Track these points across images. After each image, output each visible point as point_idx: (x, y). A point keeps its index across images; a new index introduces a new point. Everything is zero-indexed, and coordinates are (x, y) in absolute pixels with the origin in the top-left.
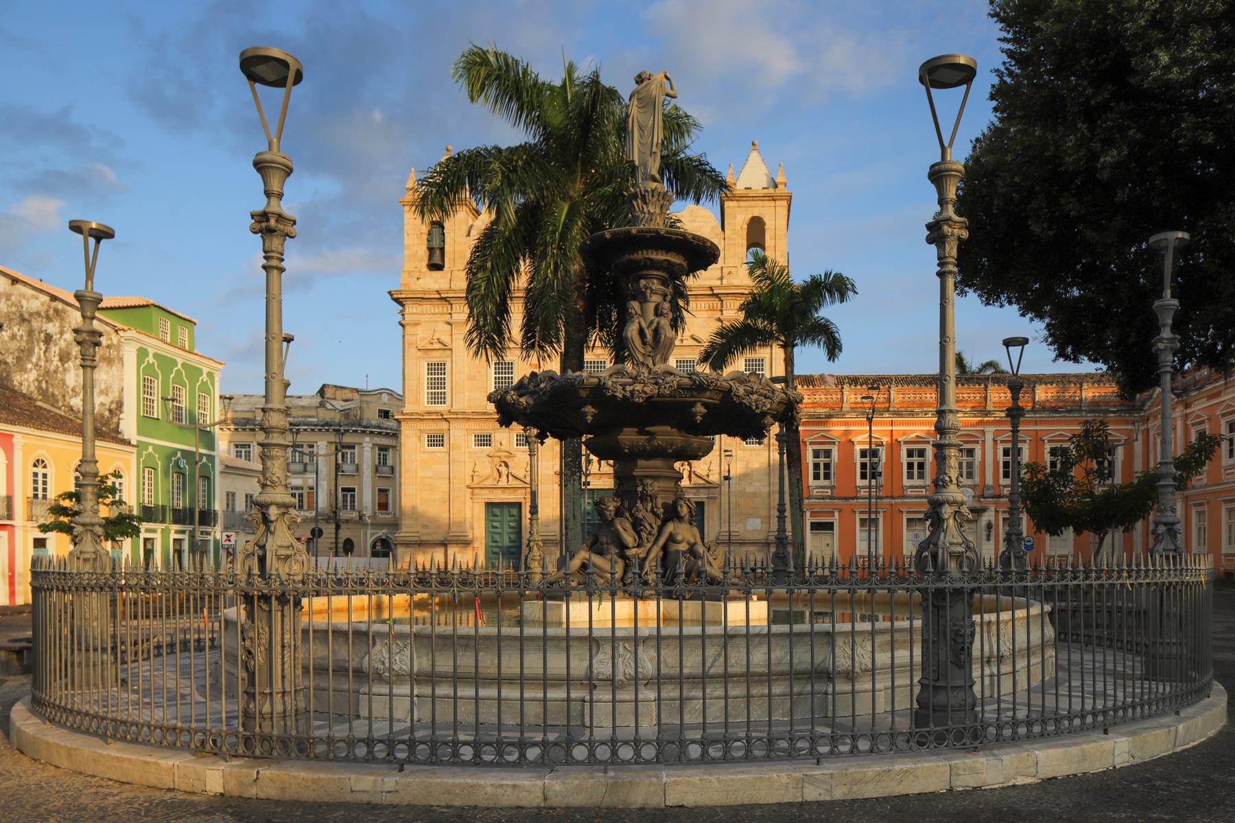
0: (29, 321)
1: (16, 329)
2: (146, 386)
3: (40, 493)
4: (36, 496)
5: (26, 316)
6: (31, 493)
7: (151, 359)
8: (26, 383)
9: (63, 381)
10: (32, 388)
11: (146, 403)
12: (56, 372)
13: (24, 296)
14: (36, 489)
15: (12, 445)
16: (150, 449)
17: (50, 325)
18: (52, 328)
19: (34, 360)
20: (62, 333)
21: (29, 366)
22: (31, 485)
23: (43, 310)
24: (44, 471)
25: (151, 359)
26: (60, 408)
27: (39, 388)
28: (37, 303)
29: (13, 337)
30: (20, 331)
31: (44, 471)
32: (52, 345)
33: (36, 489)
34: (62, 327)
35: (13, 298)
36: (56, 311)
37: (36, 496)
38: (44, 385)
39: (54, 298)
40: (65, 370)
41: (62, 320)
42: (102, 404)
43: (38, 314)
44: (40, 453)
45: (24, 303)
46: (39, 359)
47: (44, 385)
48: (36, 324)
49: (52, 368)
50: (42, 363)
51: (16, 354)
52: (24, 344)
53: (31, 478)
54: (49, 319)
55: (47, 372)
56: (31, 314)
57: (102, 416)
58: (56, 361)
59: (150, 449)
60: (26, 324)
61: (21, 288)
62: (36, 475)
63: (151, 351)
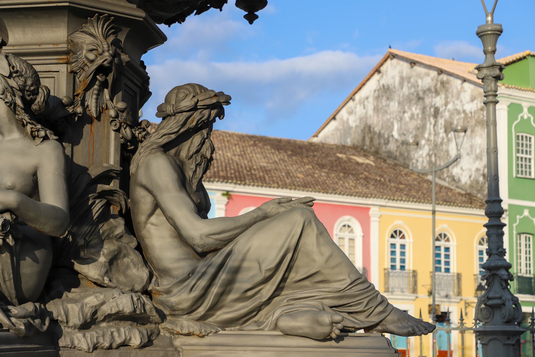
0: (423, 99)
1: (414, 109)
2: (521, 144)
3: (398, 264)
4: (393, 267)
5: (421, 94)
6: (388, 264)
7: (525, 114)
8: (420, 160)
9: (447, 151)
10: (425, 164)
11: (522, 165)
12: (442, 144)
13: (419, 76)
14: (393, 260)
15: (369, 217)
16: (526, 213)
17: (438, 98)
18: (439, 101)
19: (426, 136)
20: (446, 104)
21: (423, 142)
22: (388, 256)
23: (432, 84)
24: (402, 241)
25: (525, 114)
26: (444, 180)
27: (430, 162)
28: (427, 80)
29: (412, 117)
30: (416, 110)
31: (402, 241)
32: (439, 118)
33: (393, 260)
34: (446, 98)
35: (412, 80)
36: (443, 83)
37: (393, 267)
38: (433, 159)
39: (441, 72)
40: (449, 140)
41: (447, 91)
42: (478, 170)
43: (429, 90)
44: (398, 224)
45: (420, 82)
46: (430, 134)
47: (433, 159)
48: (427, 101)
49: (439, 140)
50: (432, 138)
51: (414, 133)
52: (419, 122)
53: (388, 250)
54: (437, 93)
55: (436, 145)
56: (424, 92)
57: (477, 182)
58: (442, 134)
59: (526, 213)
60: (421, 101)
61: (418, 69)
62: (393, 245)
63: (525, 105)
